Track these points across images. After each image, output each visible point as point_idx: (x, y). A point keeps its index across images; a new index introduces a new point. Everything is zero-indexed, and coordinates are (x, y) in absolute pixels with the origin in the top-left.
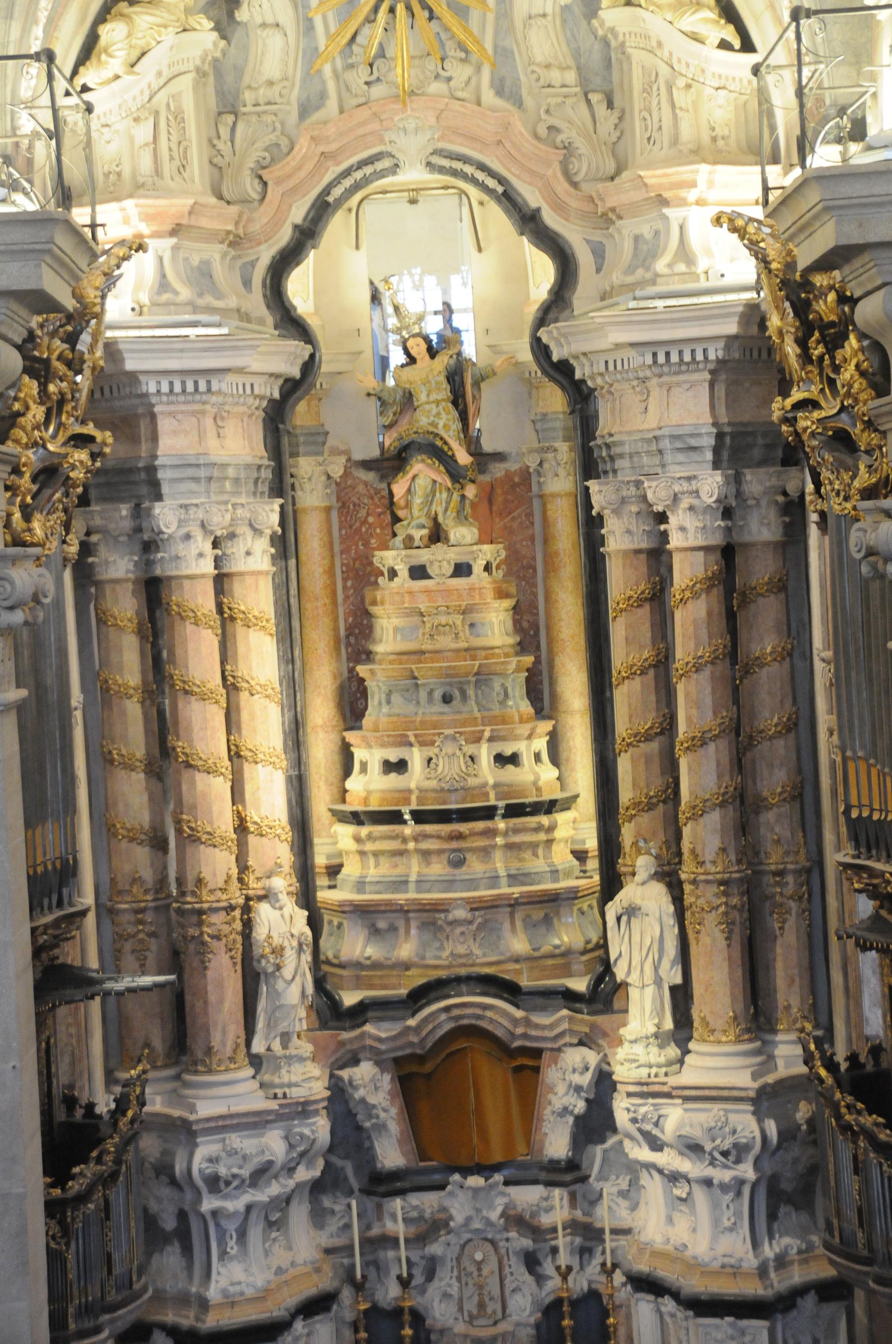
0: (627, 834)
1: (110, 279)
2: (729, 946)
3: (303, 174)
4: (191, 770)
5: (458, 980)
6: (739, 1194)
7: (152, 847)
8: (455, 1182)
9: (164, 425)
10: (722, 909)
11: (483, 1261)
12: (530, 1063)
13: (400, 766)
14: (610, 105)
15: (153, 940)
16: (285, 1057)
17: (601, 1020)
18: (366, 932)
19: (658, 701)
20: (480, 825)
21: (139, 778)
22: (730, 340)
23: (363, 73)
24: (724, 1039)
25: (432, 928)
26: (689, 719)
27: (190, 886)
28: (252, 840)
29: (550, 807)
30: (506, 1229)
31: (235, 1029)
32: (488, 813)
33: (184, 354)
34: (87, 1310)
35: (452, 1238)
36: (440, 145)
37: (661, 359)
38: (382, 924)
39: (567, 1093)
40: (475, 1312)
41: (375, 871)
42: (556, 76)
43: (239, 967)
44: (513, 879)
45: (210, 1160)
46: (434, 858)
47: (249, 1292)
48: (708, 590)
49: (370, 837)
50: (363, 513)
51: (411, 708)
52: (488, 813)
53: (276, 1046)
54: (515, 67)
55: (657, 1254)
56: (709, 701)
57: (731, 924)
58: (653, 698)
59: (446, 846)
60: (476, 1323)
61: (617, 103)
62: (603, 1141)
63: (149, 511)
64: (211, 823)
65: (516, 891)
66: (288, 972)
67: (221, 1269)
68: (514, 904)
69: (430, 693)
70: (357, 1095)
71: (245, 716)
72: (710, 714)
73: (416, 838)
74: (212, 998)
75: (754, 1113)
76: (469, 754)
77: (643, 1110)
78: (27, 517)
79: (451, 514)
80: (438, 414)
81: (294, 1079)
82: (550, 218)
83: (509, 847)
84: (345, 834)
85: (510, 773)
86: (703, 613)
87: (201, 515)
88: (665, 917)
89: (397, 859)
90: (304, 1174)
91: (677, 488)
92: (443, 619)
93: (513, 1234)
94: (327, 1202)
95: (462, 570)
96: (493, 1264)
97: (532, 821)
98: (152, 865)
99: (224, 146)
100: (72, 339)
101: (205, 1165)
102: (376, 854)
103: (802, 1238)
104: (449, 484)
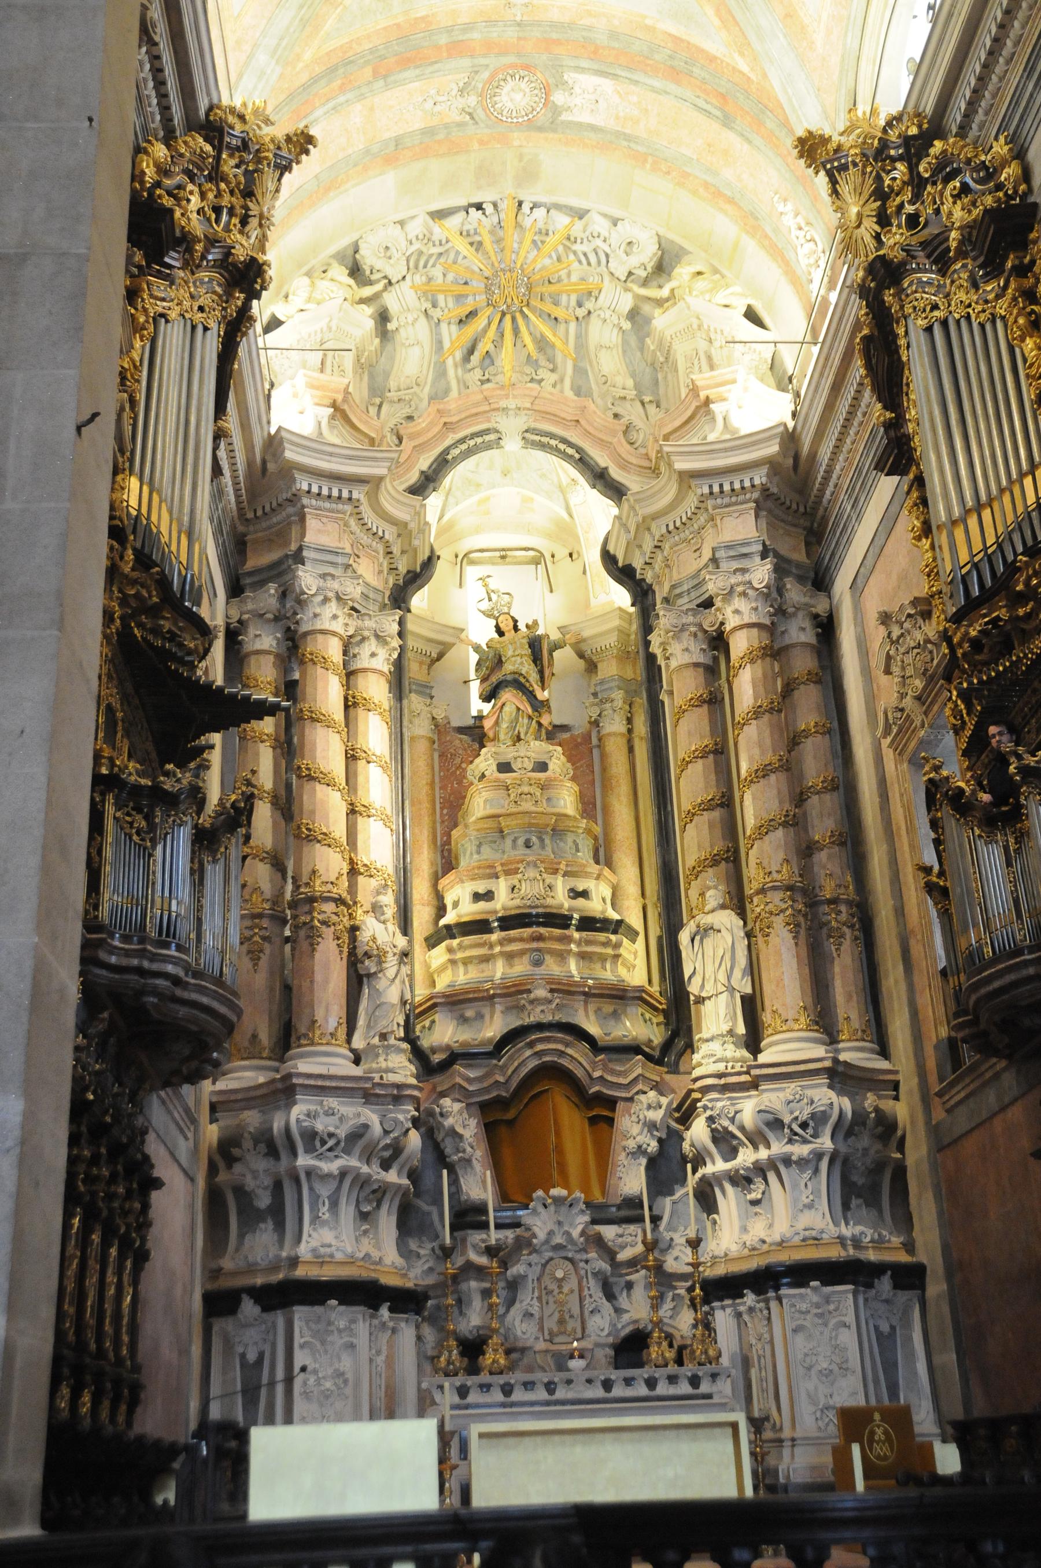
2: (796, 944)
3: (430, 435)
4: (312, 783)
5: (540, 1027)
6: (816, 1171)
7: (272, 865)
8: (538, 1198)
9: (311, 523)
10: (789, 912)
11: (563, 1279)
12: (605, 1113)
13: (488, 896)
14: (658, 406)
15: (266, 945)
16: (383, 1046)
17: (668, 1077)
18: (455, 1022)
19: (717, 781)
20: (557, 932)
22: (772, 465)
23: (478, 374)
24: (796, 1027)
25: (514, 1011)
26: (751, 759)
27: (305, 879)
28: (361, 880)
29: (617, 927)
30: (584, 1250)
33: (333, 459)
35: (534, 1258)
36: (533, 425)
37: (716, 489)
38: (470, 1013)
39: (640, 1134)
40: (555, 1329)
41: (463, 977)
42: (619, 380)
43: (345, 955)
45: (308, 1115)
46: (516, 961)
47: (339, 1256)
48: (764, 656)
49: (461, 947)
50: (458, 761)
51: (498, 856)
53: (376, 1040)
54: (588, 380)
56: (768, 742)
57: (797, 925)
58: (713, 777)
59: (527, 946)
60: (557, 1340)
61: (663, 405)
62: (671, 1193)
63: (294, 571)
64: (328, 827)
66: (391, 972)
67: (314, 1234)
69: (514, 841)
70: (448, 1122)
71: (361, 779)
72: (770, 753)
73: (501, 942)
74: (318, 977)
75: (831, 1087)
76: (548, 881)
77: (719, 1104)
79: (530, 737)
80: (522, 663)
81: (390, 1065)
82: (616, 473)
83: (583, 956)
84: (439, 955)
85: (581, 902)
86: (759, 673)
87: (335, 585)
88: (735, 930)
89: (484, 966)
90: (392, 1176)
91: (733, 580)
92: (526, 789)
93: (593, 1255)
95: (542, 767)
96: (573, 1283)
97: (602, 936)
98: (271, 881)
101: (302, 1117)
102: (466, 962)
103: (875, 1228)
104: (530, 711)
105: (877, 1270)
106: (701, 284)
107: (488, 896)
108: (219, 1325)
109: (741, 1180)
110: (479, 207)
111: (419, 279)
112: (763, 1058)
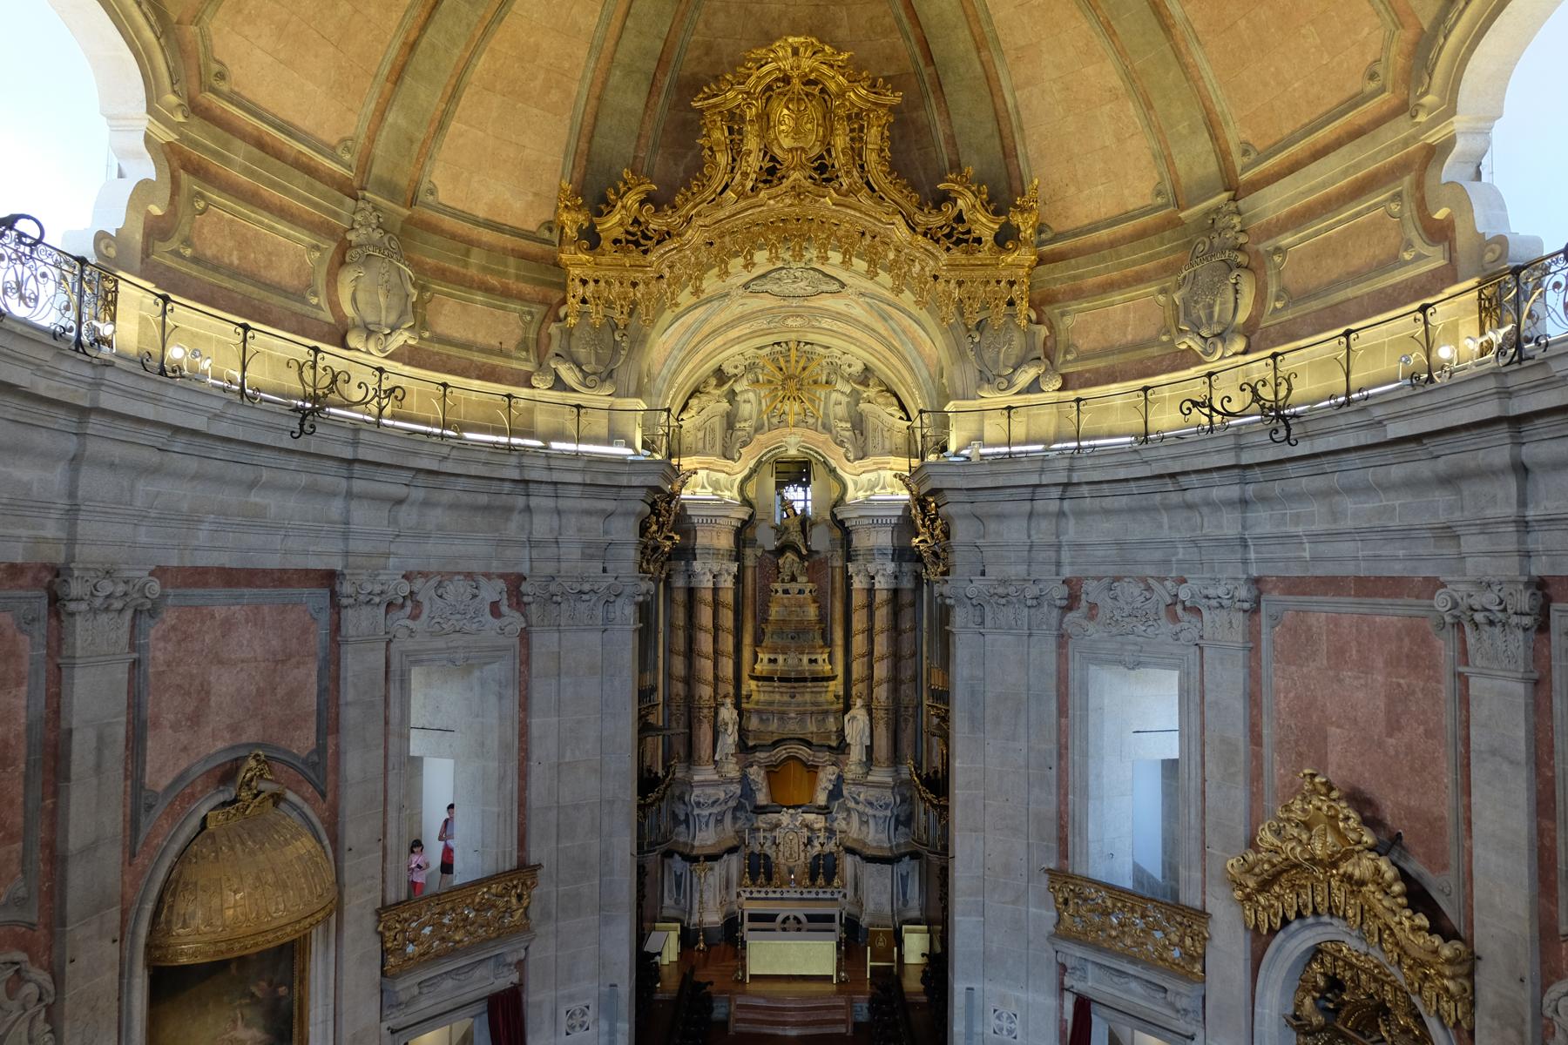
0: (854, 691)
1: (684, 483)
5: (791, 739)
9: (699, 534)
13: (775, 661)
21: (681, 658)
31: (709, 751)
32: (804, 680)
34: (651, 844)
41: (762, 697)
44: (814, 704)
52: (804, 680)
55: (854, 840)
65: (814, 708)
66: (729, 731)
68: (812, 713)
78: (648, 563)
82: (839, 471)
84: (753, 684)
85: (814, 667)
90: (732, 803)
94: (738, 814)
95: (801, 592)
97: (820, 684)
99: (728, 440)
100: (669, 503)
105: (904, 855)
106: (880, 400)
107: (775, 661)
108: (666, 861)
109: (861, 814)
110: (779, 344)
111: (751, 376)
112: (869, 778)
